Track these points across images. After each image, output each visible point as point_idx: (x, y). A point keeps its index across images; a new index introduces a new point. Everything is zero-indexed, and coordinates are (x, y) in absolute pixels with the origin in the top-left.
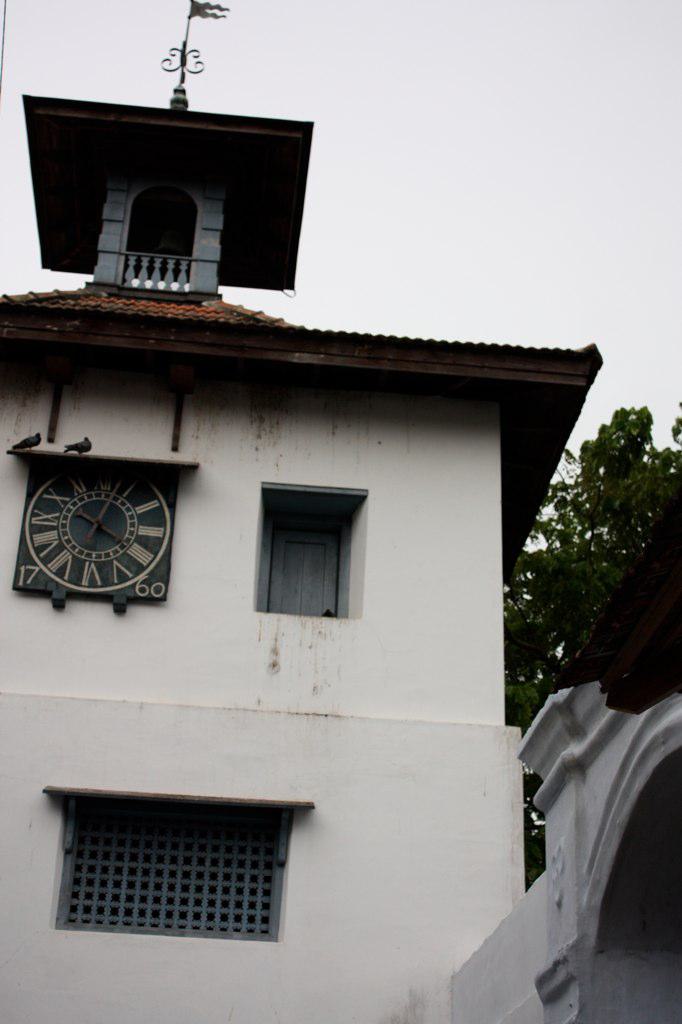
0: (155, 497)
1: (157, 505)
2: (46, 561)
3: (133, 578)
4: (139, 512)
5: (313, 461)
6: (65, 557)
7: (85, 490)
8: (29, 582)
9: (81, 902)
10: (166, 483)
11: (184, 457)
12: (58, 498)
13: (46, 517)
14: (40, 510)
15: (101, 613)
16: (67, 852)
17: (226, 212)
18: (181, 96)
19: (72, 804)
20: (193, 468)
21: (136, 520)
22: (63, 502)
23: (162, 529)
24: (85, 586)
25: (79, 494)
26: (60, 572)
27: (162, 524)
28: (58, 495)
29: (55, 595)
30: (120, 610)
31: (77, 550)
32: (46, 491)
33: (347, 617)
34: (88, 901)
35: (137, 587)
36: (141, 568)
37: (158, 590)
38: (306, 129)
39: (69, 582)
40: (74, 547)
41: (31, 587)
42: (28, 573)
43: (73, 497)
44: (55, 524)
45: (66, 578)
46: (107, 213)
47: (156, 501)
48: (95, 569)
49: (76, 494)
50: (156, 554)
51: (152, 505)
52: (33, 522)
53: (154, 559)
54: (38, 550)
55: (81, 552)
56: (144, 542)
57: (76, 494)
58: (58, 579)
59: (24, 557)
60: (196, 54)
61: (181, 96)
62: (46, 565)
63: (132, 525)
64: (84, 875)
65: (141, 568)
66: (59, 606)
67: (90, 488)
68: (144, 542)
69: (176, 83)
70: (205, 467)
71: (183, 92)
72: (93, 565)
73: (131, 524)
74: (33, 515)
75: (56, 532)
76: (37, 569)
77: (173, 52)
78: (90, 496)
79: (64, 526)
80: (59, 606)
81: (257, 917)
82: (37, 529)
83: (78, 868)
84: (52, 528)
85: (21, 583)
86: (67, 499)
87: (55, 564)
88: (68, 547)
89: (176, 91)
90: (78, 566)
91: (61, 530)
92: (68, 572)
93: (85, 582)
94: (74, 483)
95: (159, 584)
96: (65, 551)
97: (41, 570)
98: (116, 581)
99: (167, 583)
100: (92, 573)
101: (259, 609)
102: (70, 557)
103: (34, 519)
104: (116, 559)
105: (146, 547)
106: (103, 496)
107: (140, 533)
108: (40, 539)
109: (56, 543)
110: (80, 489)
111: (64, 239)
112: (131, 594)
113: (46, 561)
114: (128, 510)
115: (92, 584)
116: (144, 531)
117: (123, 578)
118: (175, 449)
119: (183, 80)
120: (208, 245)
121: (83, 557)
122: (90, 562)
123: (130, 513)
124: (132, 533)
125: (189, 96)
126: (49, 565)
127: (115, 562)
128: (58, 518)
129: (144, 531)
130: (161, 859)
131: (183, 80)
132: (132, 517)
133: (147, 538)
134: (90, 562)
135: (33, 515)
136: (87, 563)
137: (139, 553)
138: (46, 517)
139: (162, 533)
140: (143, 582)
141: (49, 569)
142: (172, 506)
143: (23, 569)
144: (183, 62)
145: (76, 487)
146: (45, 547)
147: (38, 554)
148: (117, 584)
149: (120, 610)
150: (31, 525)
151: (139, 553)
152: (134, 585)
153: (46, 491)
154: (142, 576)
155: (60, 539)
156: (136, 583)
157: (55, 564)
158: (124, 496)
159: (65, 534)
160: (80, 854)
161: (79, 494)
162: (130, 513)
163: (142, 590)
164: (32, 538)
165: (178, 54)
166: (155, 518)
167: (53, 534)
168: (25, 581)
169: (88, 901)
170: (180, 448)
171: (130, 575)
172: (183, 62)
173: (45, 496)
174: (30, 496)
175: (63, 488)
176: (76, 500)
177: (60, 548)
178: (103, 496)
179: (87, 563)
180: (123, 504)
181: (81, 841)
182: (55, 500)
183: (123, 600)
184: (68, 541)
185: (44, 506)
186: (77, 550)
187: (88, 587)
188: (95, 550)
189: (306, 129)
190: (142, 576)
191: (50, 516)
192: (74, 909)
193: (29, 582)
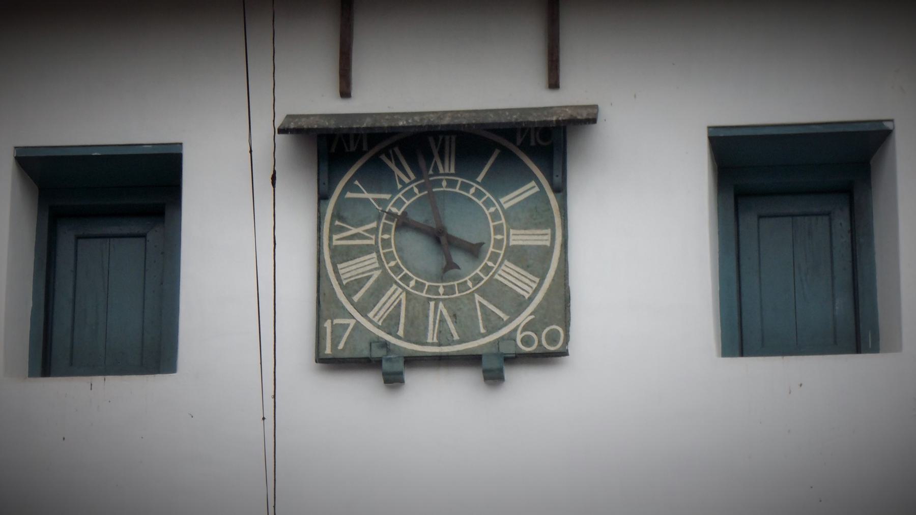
0: (533, 177)
1: (537, 189)
2: (363, 309)
3: (510, 321)
4: (506, 206)
6: (394, 296)
7: (413, 177)
8: (341, 346)
10: (540, 147)
11: (572, 94)
12: (370, 196)
13: (354, 231)
14: (341, 219)
21: (503, 221)
22: (379, 201)
23: (549, 231)
24: (433, 344)
25: (405, 185)
26: (390, 325)
27: (551, 224)
28: (369, 191)
29: (386, 366)
30: (494, 378)
31: (412, 283)
32: (349, 187)
33: (875, 349)
35: (519, 337)
36: (520, 304)
39: (407, 339)
40: (406, 279)
41: (346, 355)
42: (338, 331)
43: (394, 191)
44: (373, 242)
45: (401, 333)
47: (533, 183)
48: (445, 312)
49: (399, 186)
50: (543, 279)
51: (529, 190)
52: (335, 243)
53: (540, 285)
55: (419, 286)
56: (518, 256)
57: (399, 186)
58: (388, 338)
59: (324, 304)
62: (365, 315)
63: (498, 230)
65: (520, 304)
66: (393, 380)
67: (419, 174)
68: (518, 256)
70: (605, 113)
72: (441, 305)
73: (495, 227)
74: (333, 230)
75: (374, 255)
76: (352, 323)
80: (393, 380)
82: (342, 255)
85: (328, 351)
86: (387, 196)
87: (380, 311)
88: (397, 279)
91: (381, 251)
92: (402, 320)
93: (431, 337)
94: (392, 165)
95: (554, 327)
96: (394, 286)
97: (358, 322)
98: (483, 331)
99: (566, 323)
100: (443, 320)
102: (403, 297)
103: (335, 237)
104: (477, 291)
105: (526, 268)
106: (444, 183)
107: (512, 243)
108: (350, 269)
109: (376, 274)
110: (404, 176)
113: (363, 309)
114: (488, 203)
115: (444, 338)
116: (520, 238)
121: (424, 294)
122: (437, 301)
123: (492, 209)
124: (498, 244)
126: (371, 315)
127: (478, 298)
128: (374, 231)
129: (520, 238)
132: (495, 216)
134: (437, 301)
135: (333, 230)
136: (432, 304)
138: (354, 231)
139: (548, 237)
140: (525, 329)
141: (371, 321)
142: (560, 190)
143: (328, 325)
145: (398, 172)
146: (360, 283)
147: (349, 297)
148: (484, 336)
149: (494, 378)
150: (334, 250)
152: (511, 337)
153: (349, 187)
154: (525, 317)
155: (382, 266)
156: (515, 330)
157: (380, 311)
158: (479, 179)
159: (389, 257)
161: (405, 185)
162: (492, 209)
163: (527, 341)
164: (336, 271)
166: (538, 215)
167: (370, 260)
168: (335, 345)
170: (561, 84)
171: (505, 317)
173: (349, 195)
174: (323, 197)
175: (376, 175)
176: (400, 195)
178: (444, 183)
179: (432, 304)
180: (479, 194)
182: (367, 201)
186: (412, 283)
187: (440, 345)
188: (443, 281)
190: (525, 317)
191: (360, 230)
193: (341, 346)
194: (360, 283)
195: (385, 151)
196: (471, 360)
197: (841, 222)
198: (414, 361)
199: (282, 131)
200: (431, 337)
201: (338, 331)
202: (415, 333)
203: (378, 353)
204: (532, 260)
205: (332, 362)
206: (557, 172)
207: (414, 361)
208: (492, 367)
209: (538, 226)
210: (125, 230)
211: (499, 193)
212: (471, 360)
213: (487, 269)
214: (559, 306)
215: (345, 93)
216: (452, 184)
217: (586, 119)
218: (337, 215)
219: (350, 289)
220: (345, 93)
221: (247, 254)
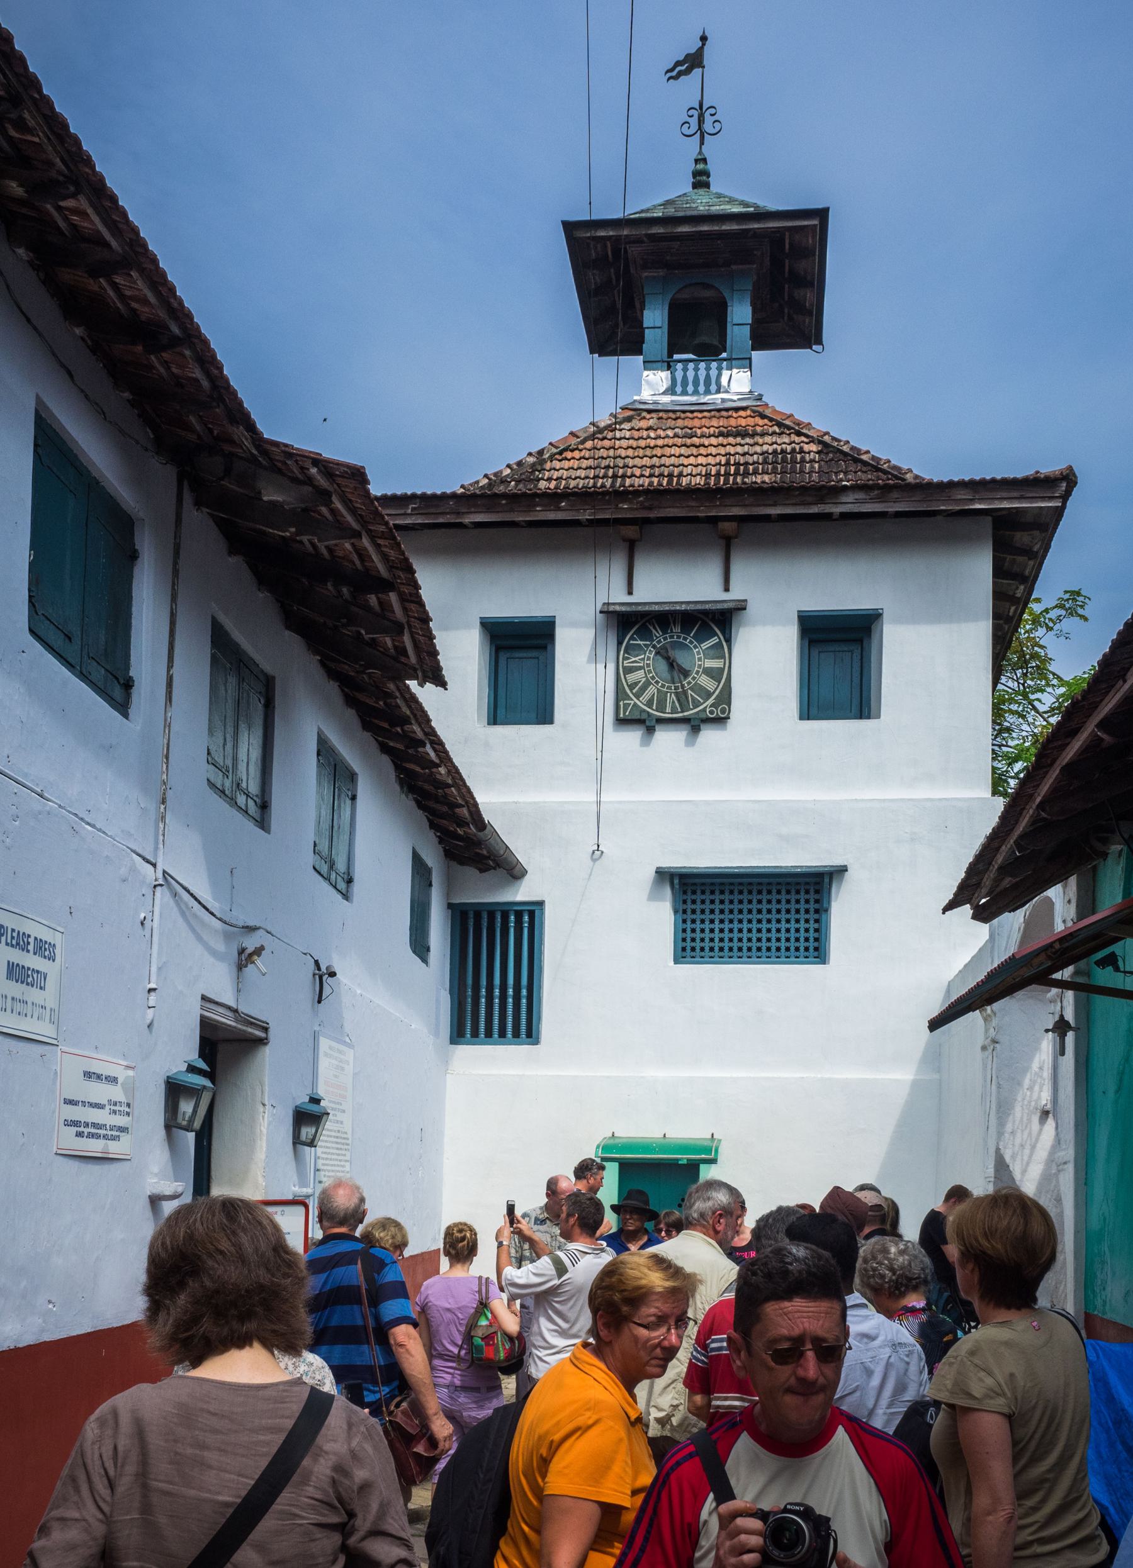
2: (638, 696)
5: (838, 584)
6: (652, 690)
9: (689, 944)
10: (717, 622)
16: (676, 912)
17: (753, 304)
18: (701, 166)
19: (676, 881)
20: (741, 607)
26: (649, 703)
29: (648, 723)
32: (632, 638)
33: (869, 717)
36: (709, 695)
37: (723, 711)
40: (657, 682)
42: (626, 706)
51: (714, 641)
54: (631, 687)
55: (663, 686)
56: (708, 672)
59: (620, 695)
60: (712, 111)
61: (701, 166)
63: (700, 659)
64: (689, 926)
65: (709, 695)
66: (650, 730)
67: (665, 632)
68: (708, 672)
69: (695, 155)
71: (704, 160)
74: (625, 659)
77: (691, 113)
78: (665, 639)
79: (648, 665)
81: (815, 950)
82: (629, 670)
83: (684, 921)
84: (640, 668)
87: (645, 697)
89: (697, 161)
93: (668, 710)
101: (801, 718)
108: (632, 678)
110: (657, 633)
111: (611, 331)
112: (704, 716)
113: (638, 696)
114: (695, 647)
117: (696, 704)
118: (727, 589)
119: (702, 143)
124: (700, 666)
125: (710, 167)
128: (643, 659)
130: (740, 912)
131: (702, 143)
133: (711, 669)
135: (625, 659)
137: (705, 681)
142: (729, 641)
144: (701, 120)
146: (636, 684)
147: (631, 690)
151: (705, 681)
152: (704, 710)
153: (632, 638)
154: (711, 701)
157: (645, 697)
159: (650, 672)
160: (684, 912)
163: (711, 712)
165: (696, 113)
166: (718, 651)
172: (701, 120)
174: (620, 643)
175: (644, 633)
177: (647, 684)
180: (691, 642)
181: (685, 902)
183: (696, 723)
184: (653, 678)
185: (634, 660)
190: (711, 701)
192: (684, 949)
194: (636, 684)
195: (648, 621)
196: (685, 721)
197: (857, 653)
198: (660, 721)
199: (601, 612)
200: (668, 710)
201: (626, 706)
202: (661, 708)
203: (644, 716)
205: (622, 722)
206: (727, 631)
207: (660, 721)
208: (695, 725)
209: (718, 658)
210: (530, 655)
211: (701, 642)
212: (685, 721)
213: (694, 678)
214: (725, 697)
215: (630, 593)
216: (679, 637)
217: (741, 607)
218: (626, 651)
219: (631, 687)
220: (630, 593)
221: (583, 670)
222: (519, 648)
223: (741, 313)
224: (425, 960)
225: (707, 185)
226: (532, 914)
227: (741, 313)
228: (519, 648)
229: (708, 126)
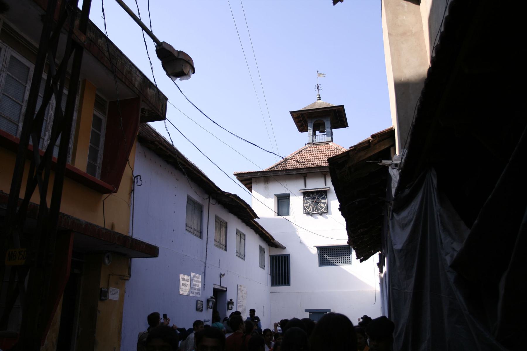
15: (319, 216)
30: (321, 215)
34: (323, 262)
38: (343, 106)
46: (309, 128)
59: (304, 209)
65: (322, 208)
80: (311, 215)
82: (306, 203)
90: (313, 208)
116: (323, 201)
120: (328, 130)
129: (323, 201)
142: (326, 196)
157: (309, 209)
166: (324, 198)
169: (323, 262)
175: (308, 196)
177: (310, 206)
189: (343, 106)
196: (318, 213)
204: (324, 203)
207: (313, 214)
208: (321, 214)
212: (318, 213)
214: (327, 208)
222: (283, 200)
223: (328, 124)
224: (264, 269)
225: (320, 99)
226: (287, 257)
227: (328, 124)
228: (283, 200)
229: (319, 88)
